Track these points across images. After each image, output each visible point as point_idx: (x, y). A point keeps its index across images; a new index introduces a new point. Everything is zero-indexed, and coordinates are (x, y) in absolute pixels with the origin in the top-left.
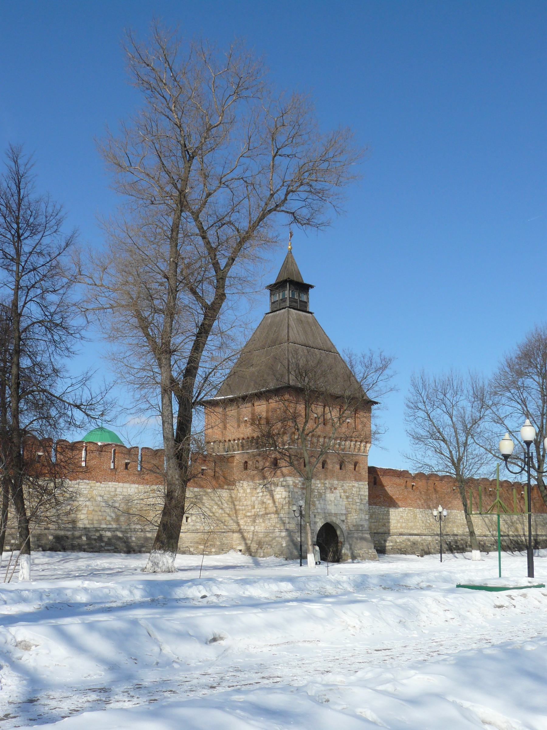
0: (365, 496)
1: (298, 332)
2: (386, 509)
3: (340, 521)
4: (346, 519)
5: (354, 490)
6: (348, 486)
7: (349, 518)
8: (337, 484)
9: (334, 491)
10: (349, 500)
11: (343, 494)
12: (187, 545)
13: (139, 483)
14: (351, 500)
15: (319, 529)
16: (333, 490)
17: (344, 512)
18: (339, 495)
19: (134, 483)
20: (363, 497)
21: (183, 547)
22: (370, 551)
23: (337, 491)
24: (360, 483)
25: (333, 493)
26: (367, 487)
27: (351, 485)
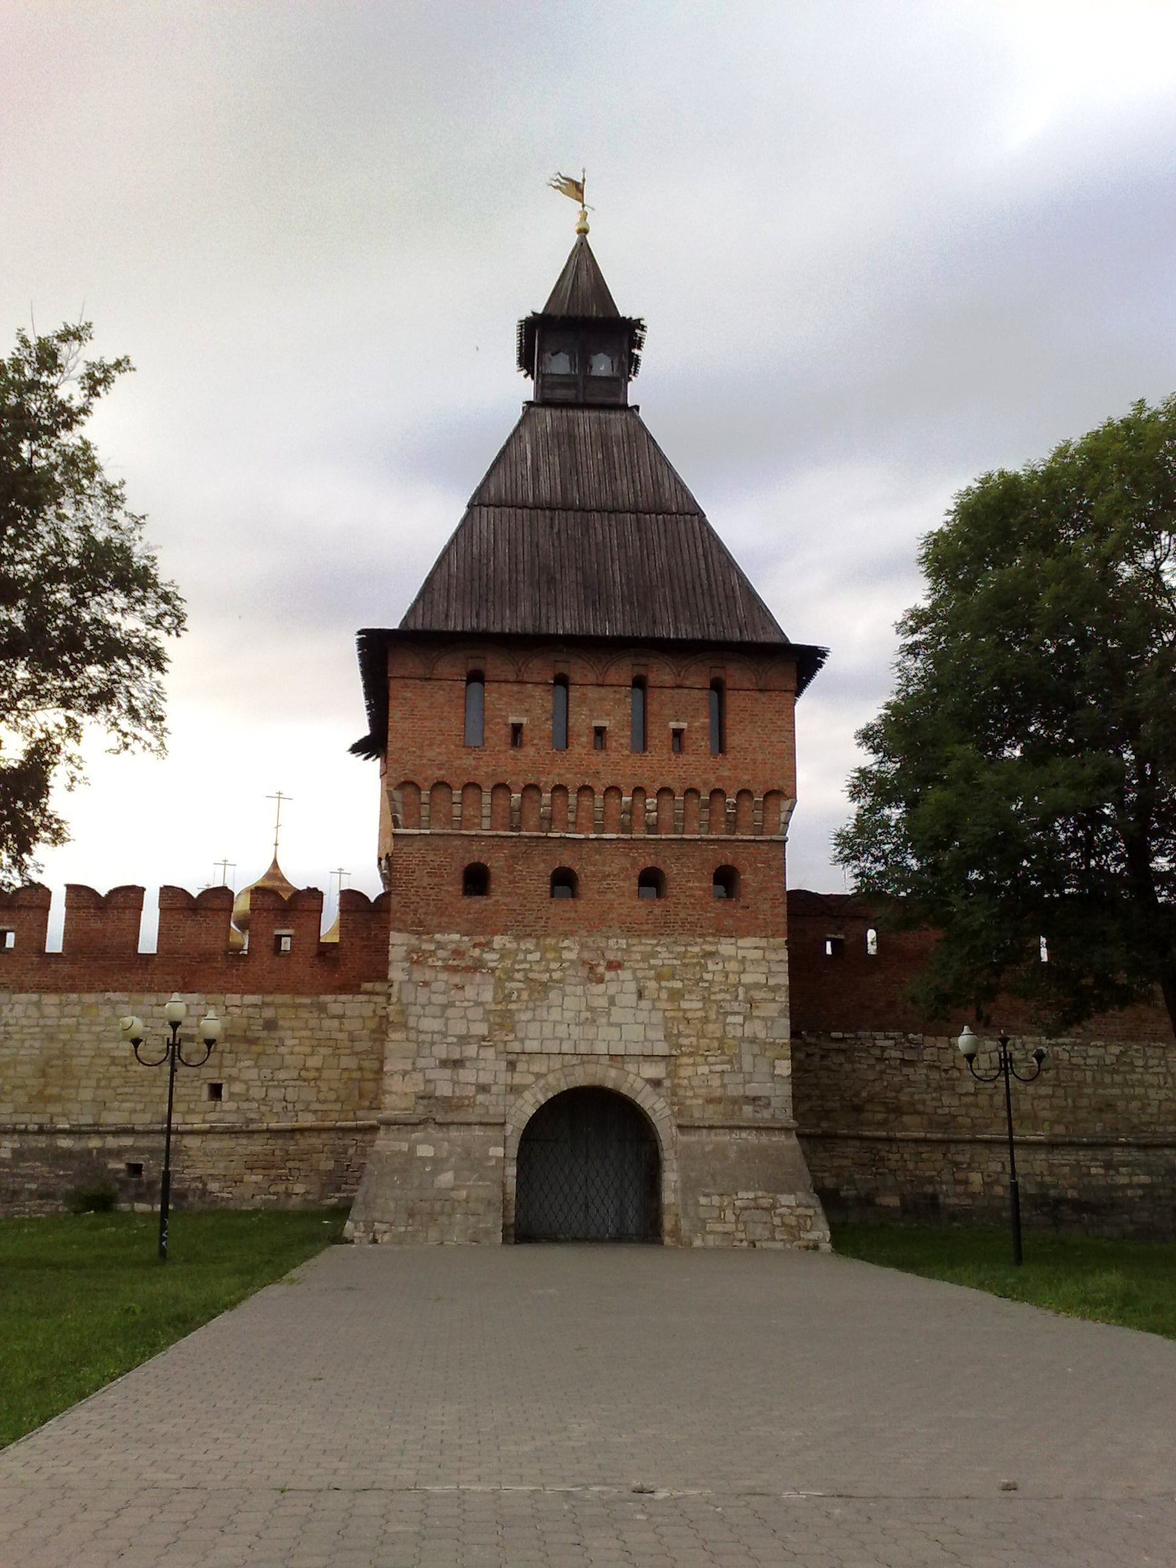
0: (775, 989)
1: (536, 470)
2: (1115, 1049)
3: (639, 1084)
4: (671, 1074)
5: (711, 967)
6: (684, 955)
7: (684, 1072)
8: (627, 950)
9: (609, 975)
10: (685, 1005)
11: (652, 984)
12: (198, 1172)
13: (41, 989)
14: (700, 1005)
15: (531, 1111)
16: (601, 970)
17: (662, 1049)
18: (632, 987)
19: (22, 989)
20: (758, 995)
21: (183, 1180)
22: (787, 1199)
23: (625, 975)
24: (741, 943)
25: (601, 980)
26: (784, 955)
27: (696, 949)
